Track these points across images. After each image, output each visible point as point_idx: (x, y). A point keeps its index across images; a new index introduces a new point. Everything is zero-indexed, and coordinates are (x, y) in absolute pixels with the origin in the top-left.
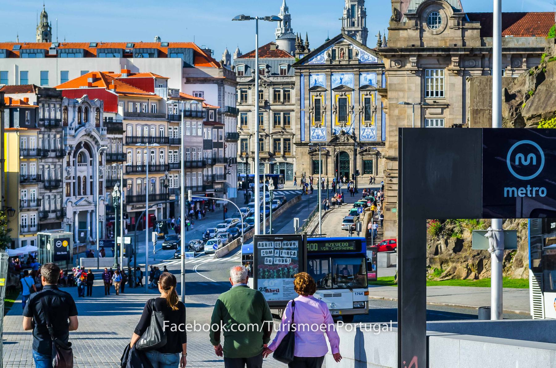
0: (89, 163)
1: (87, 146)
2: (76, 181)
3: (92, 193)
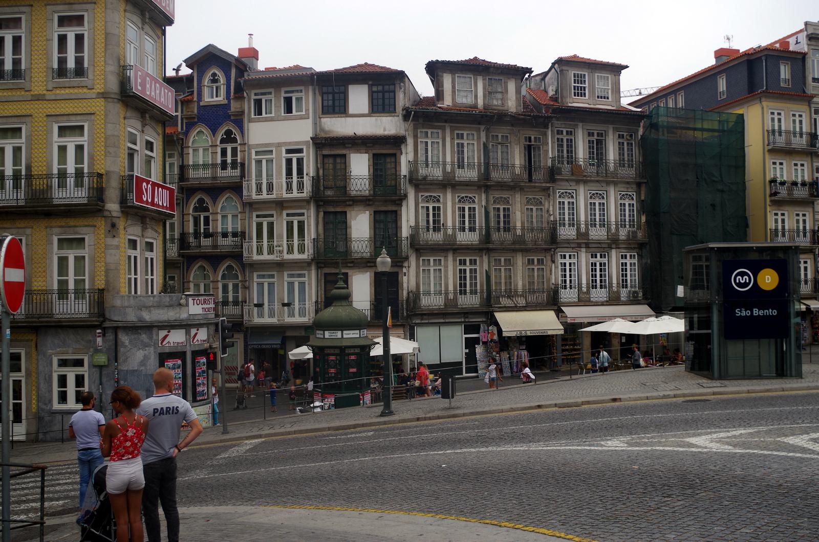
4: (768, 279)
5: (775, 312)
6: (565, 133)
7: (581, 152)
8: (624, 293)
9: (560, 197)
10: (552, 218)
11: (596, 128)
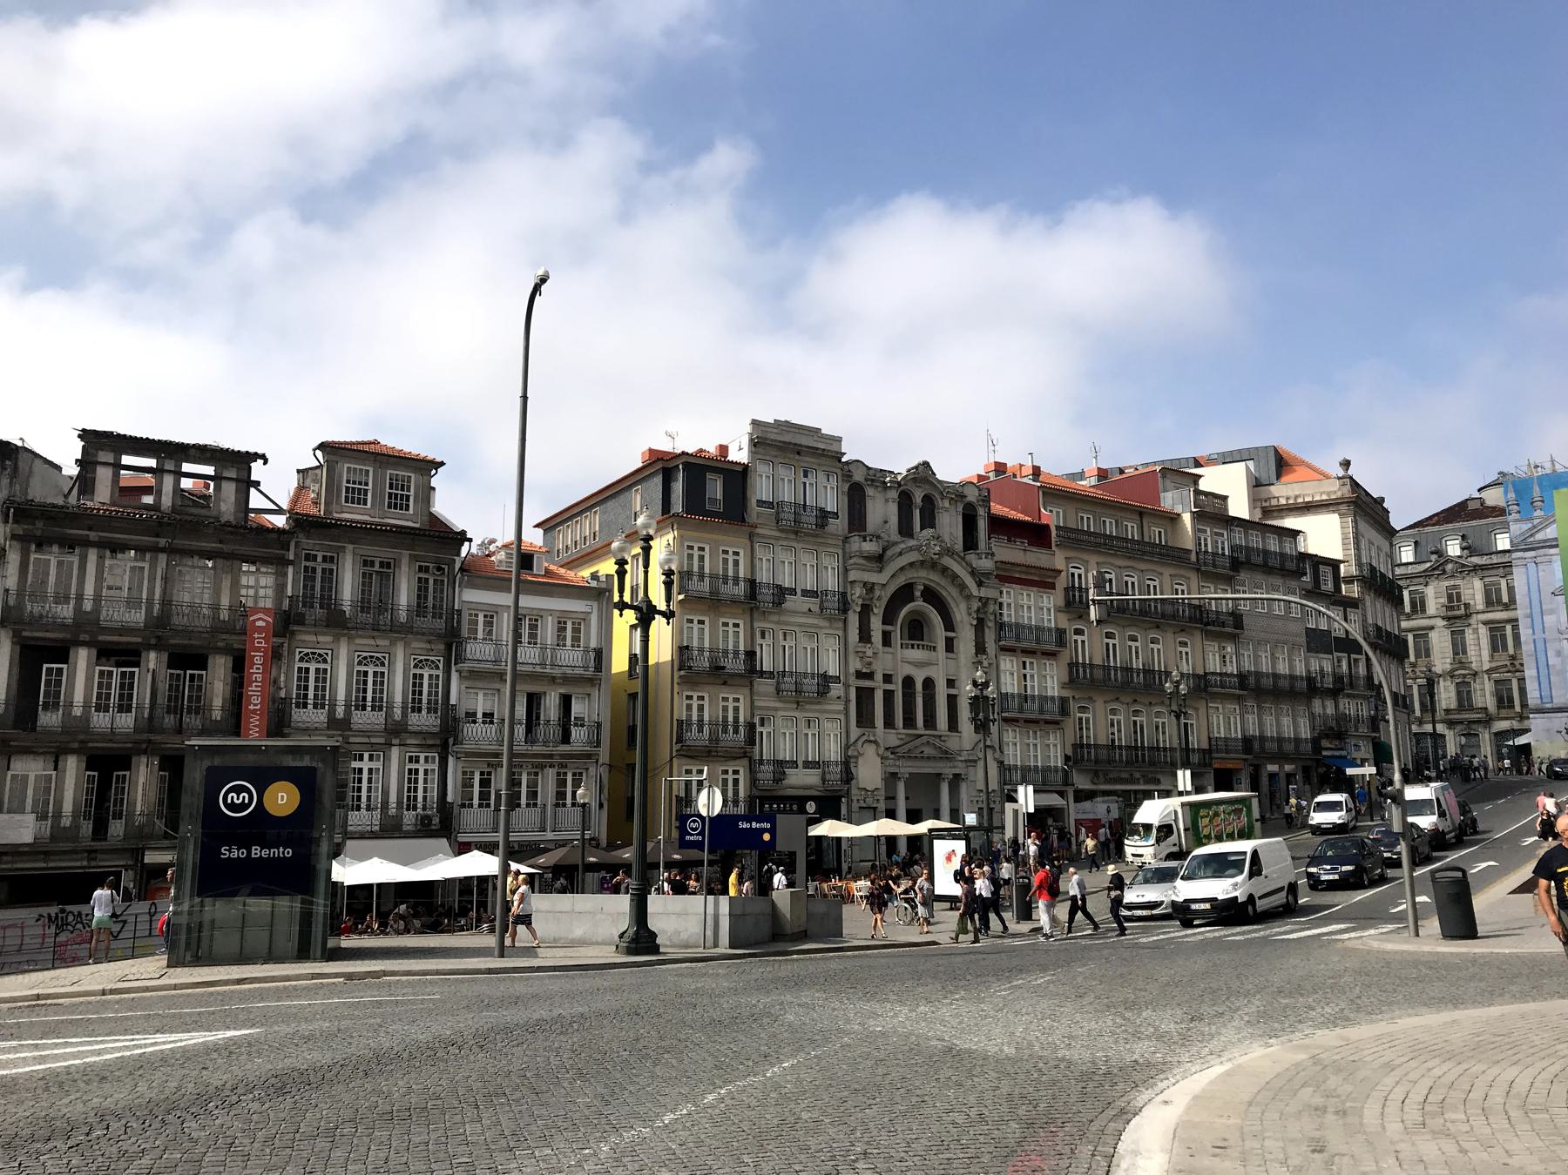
0: (941, 645)
1: (931, 596)
2: (897, 686)
3: (953, 725)
4: (282, 799)
5: (289, 853)
6: (319, 559)
7: (348, 589)
8: (409, 818)
9: (301, 660)
10: (282, 694)
11: (380, 553)
